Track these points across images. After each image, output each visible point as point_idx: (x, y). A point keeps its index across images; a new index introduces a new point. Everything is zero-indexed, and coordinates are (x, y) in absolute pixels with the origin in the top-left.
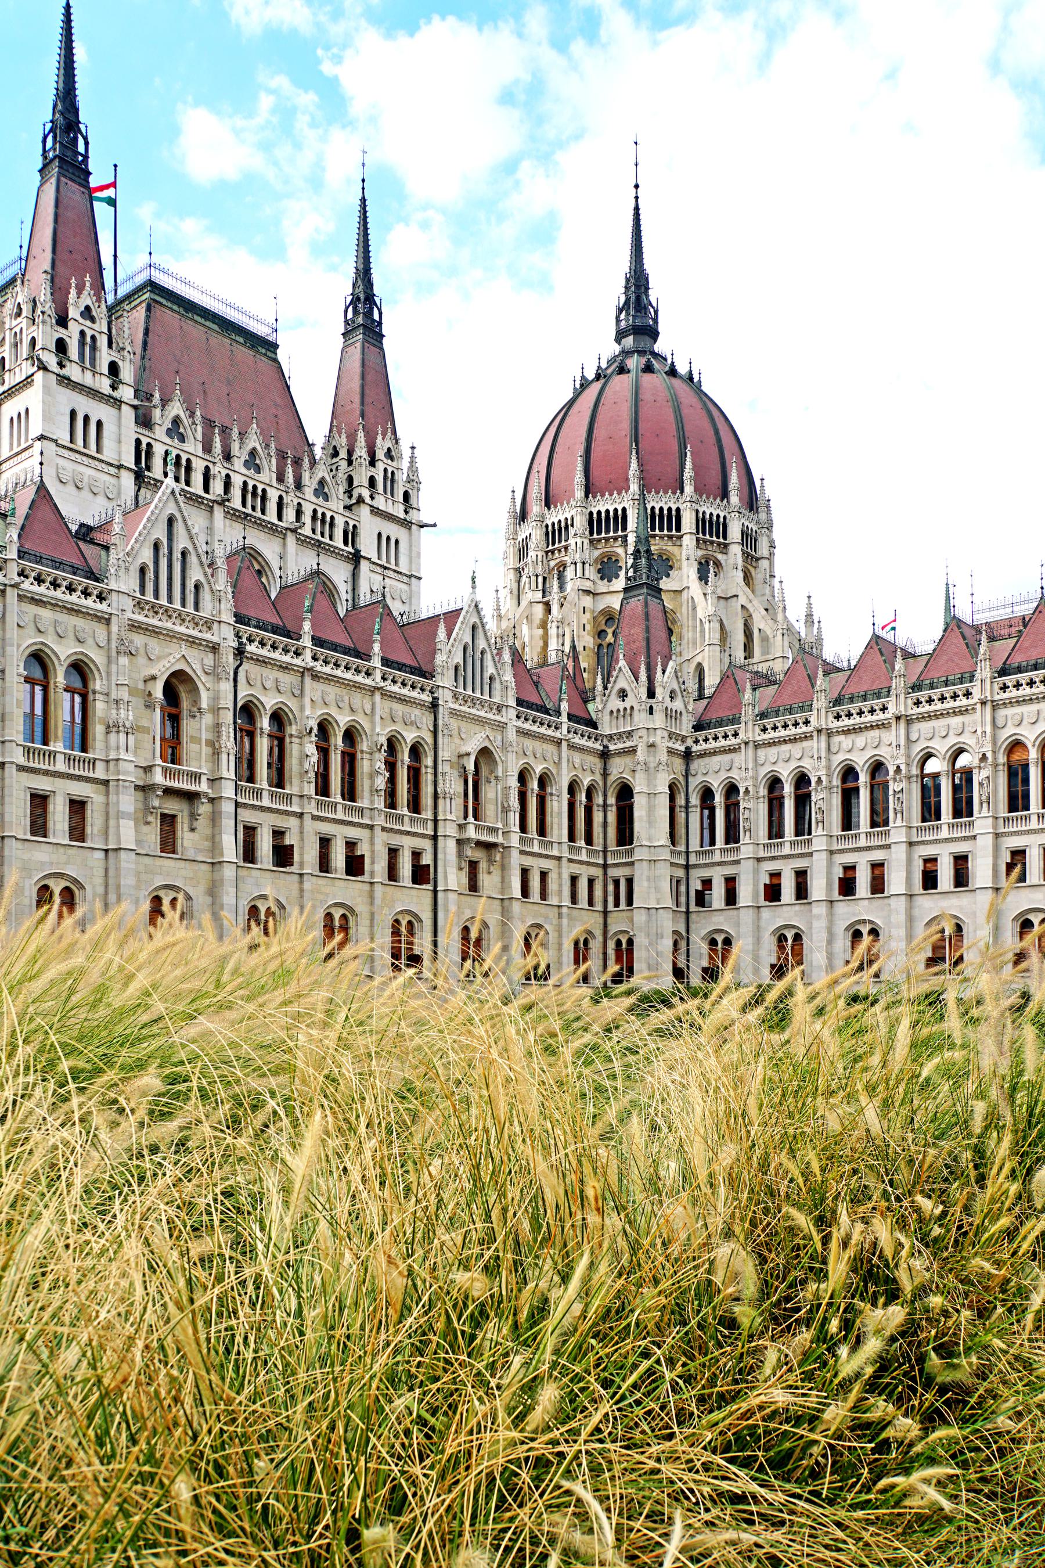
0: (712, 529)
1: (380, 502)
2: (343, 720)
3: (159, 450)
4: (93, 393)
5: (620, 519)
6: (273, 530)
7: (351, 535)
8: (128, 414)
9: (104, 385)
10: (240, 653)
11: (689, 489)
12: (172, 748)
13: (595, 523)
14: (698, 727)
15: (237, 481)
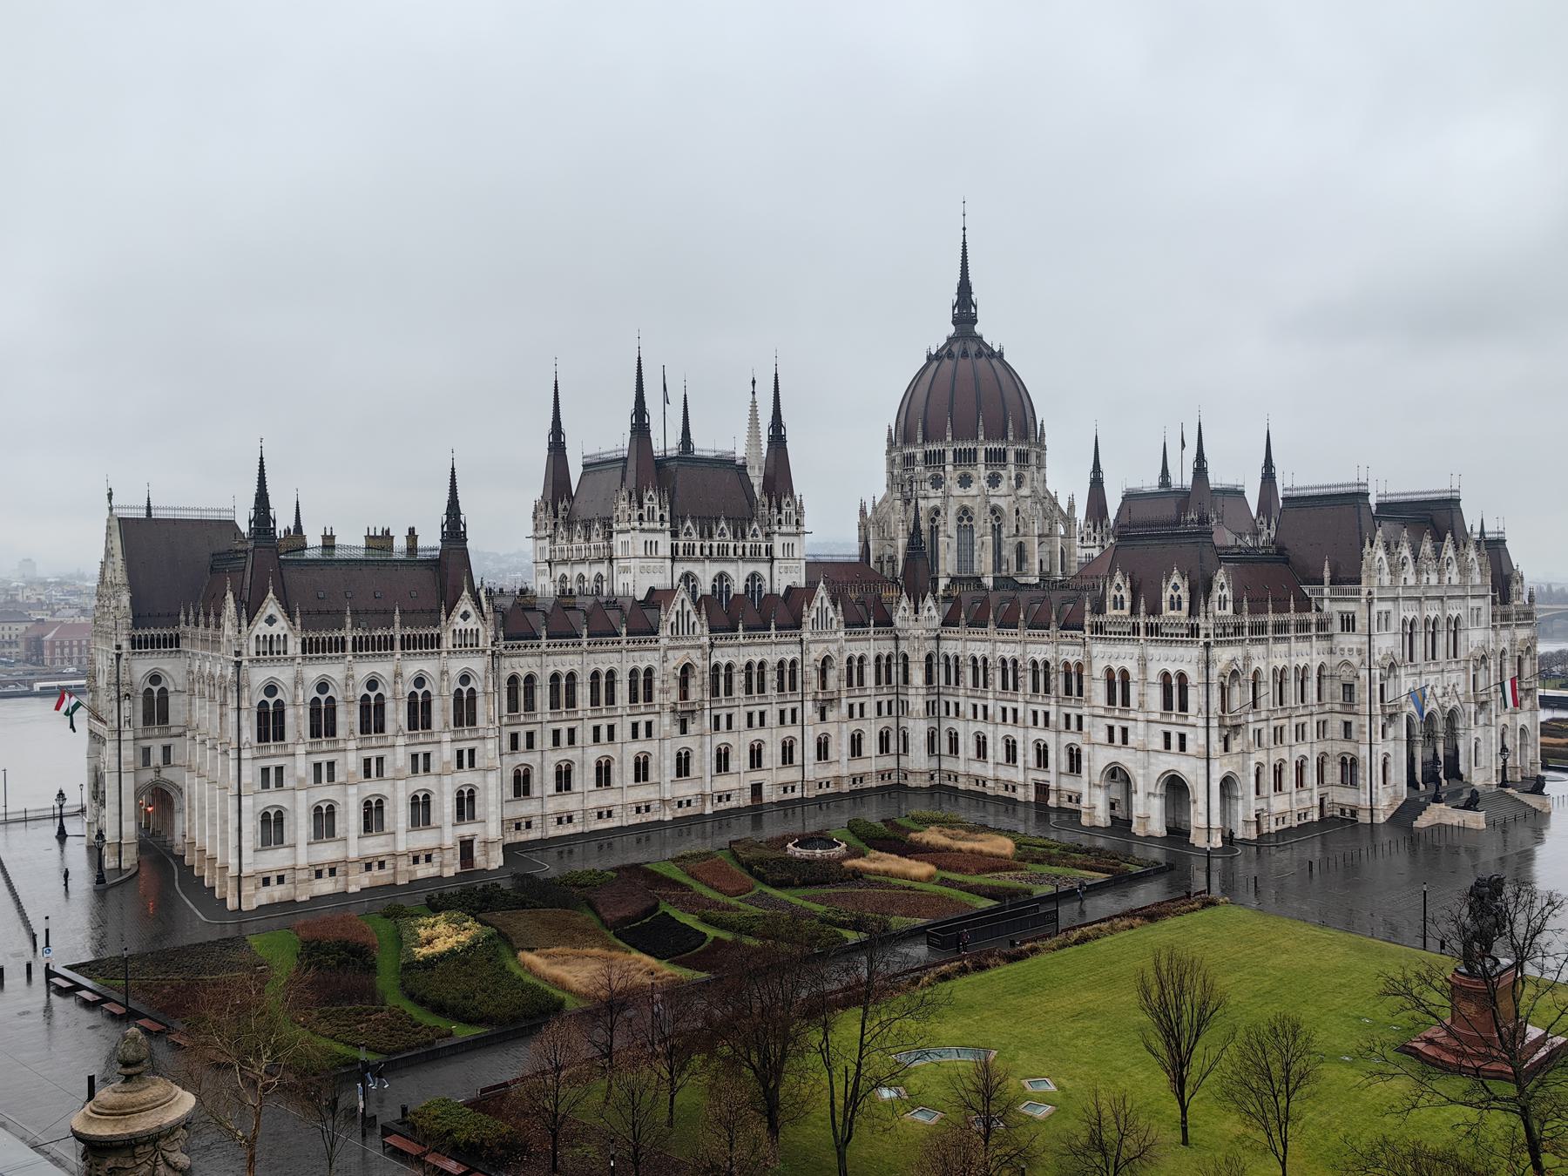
0: (997, 457)
1: (784, 529)
2: (757, 660)
3: (681, 544)
4: (654, 531)
5: (942, 454)
6: (732, 561)
7: (769, 550)
8: (668, 534)
9: (658, 526)
10: (712, 646)
11: (981, 438)
12: (684, 695)
13: (928, 457)
14: (943, 624)
15: (715, 544)
